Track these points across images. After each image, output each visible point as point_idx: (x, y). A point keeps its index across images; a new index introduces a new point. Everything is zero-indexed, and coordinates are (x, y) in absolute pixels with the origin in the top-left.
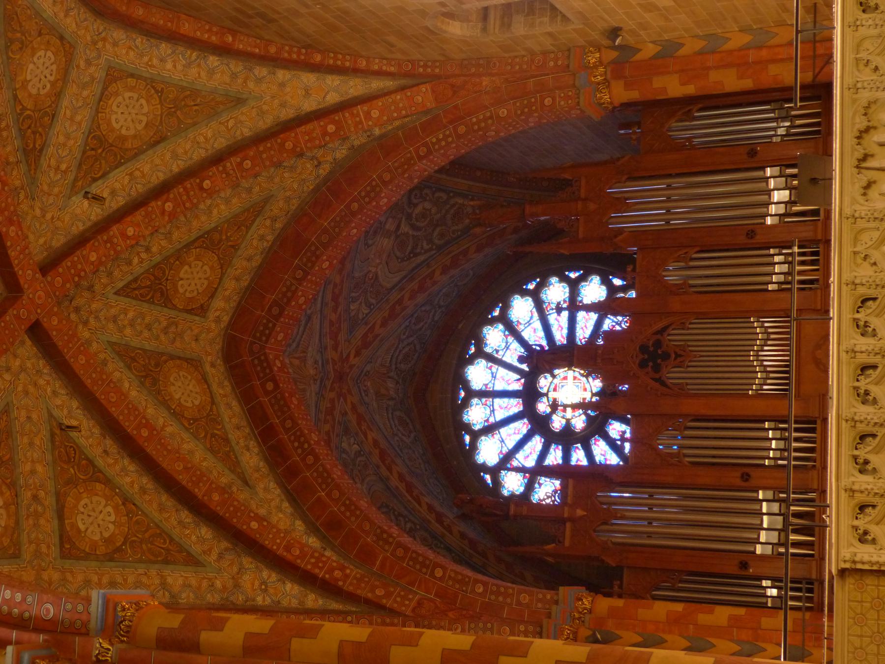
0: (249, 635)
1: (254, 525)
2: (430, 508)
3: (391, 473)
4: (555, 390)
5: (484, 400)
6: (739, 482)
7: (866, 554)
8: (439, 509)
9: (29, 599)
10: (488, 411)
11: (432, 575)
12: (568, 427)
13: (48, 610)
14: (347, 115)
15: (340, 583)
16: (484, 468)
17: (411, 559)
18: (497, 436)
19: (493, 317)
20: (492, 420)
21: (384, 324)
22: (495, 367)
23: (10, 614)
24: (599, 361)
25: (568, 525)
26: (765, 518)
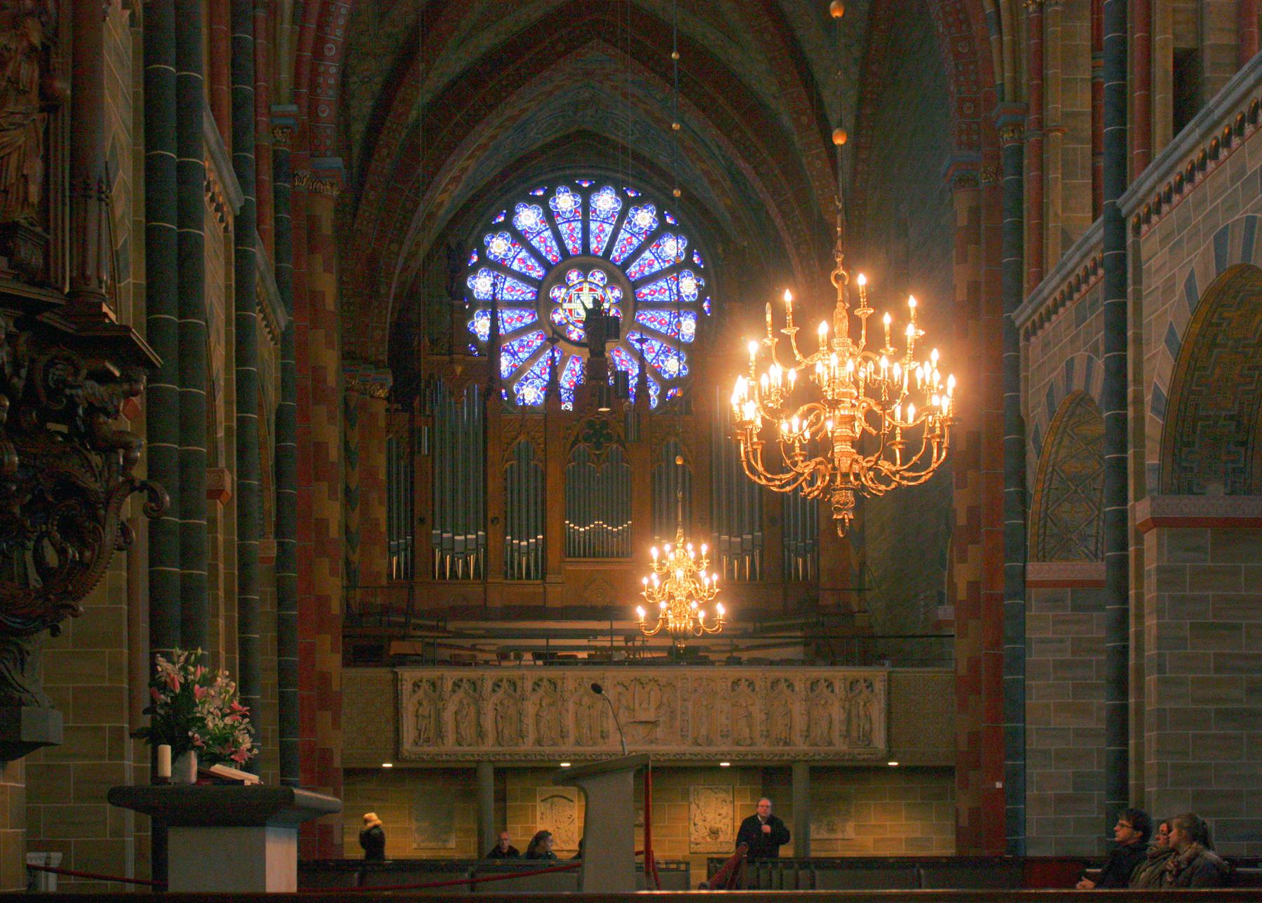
0: (323, 294)
1: (422, 66)
2: (464, 170)
3: (497, 128)
4: (591, 290)
5: (580, 210)
6: (490, 515)
7: (407, 687)
8: (464, 177)
9: (331, 92)
10: (568, 215)
11: (392, 241)
12: (554, 304)
13: (323, 112)
14: (817, 136)
15: (376, 157)
16: (511, 214)
17: (404, 218)
18: (541, 226)
19: (665, 215)
20: (560, 220)
21: (648, 112)
22: (614, 221)
23: (319, 74)
24: (594, 382)
25: (447, 358)
26: (463, 537)
